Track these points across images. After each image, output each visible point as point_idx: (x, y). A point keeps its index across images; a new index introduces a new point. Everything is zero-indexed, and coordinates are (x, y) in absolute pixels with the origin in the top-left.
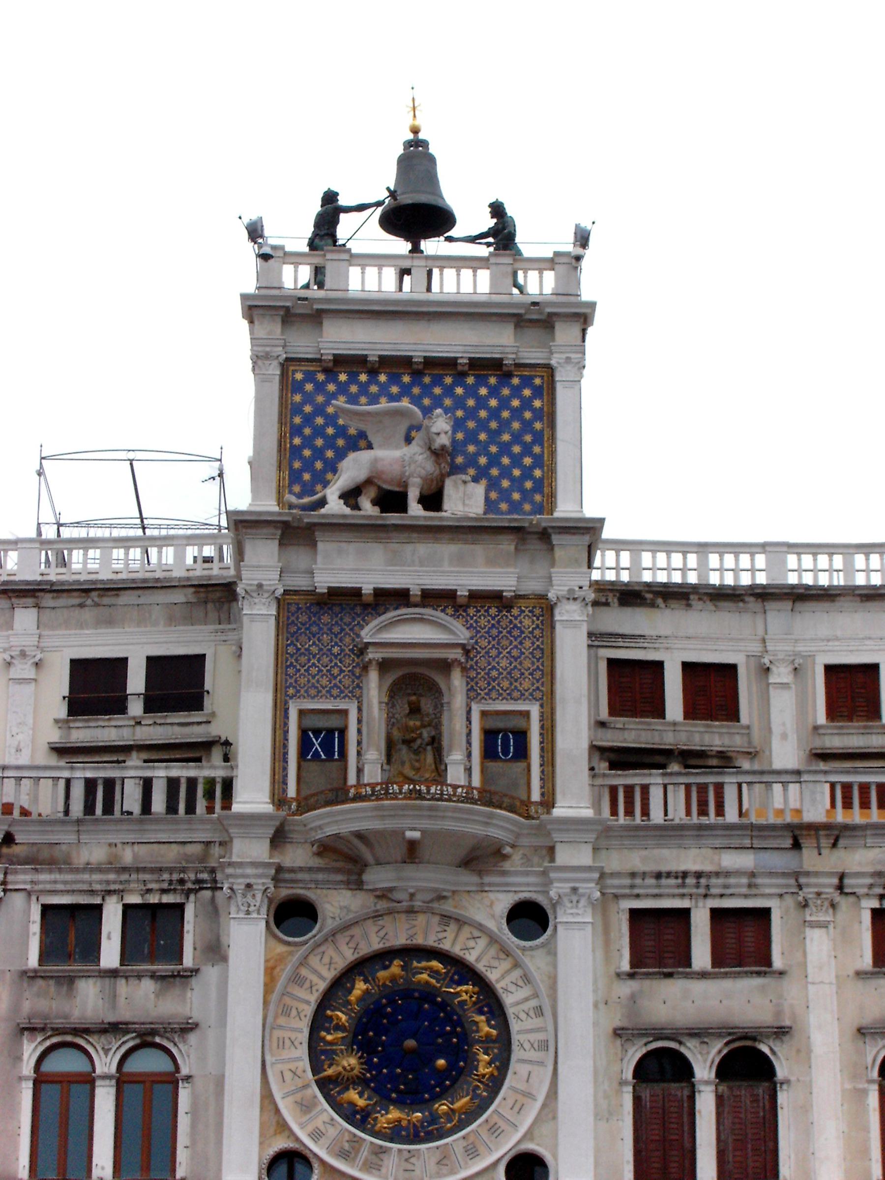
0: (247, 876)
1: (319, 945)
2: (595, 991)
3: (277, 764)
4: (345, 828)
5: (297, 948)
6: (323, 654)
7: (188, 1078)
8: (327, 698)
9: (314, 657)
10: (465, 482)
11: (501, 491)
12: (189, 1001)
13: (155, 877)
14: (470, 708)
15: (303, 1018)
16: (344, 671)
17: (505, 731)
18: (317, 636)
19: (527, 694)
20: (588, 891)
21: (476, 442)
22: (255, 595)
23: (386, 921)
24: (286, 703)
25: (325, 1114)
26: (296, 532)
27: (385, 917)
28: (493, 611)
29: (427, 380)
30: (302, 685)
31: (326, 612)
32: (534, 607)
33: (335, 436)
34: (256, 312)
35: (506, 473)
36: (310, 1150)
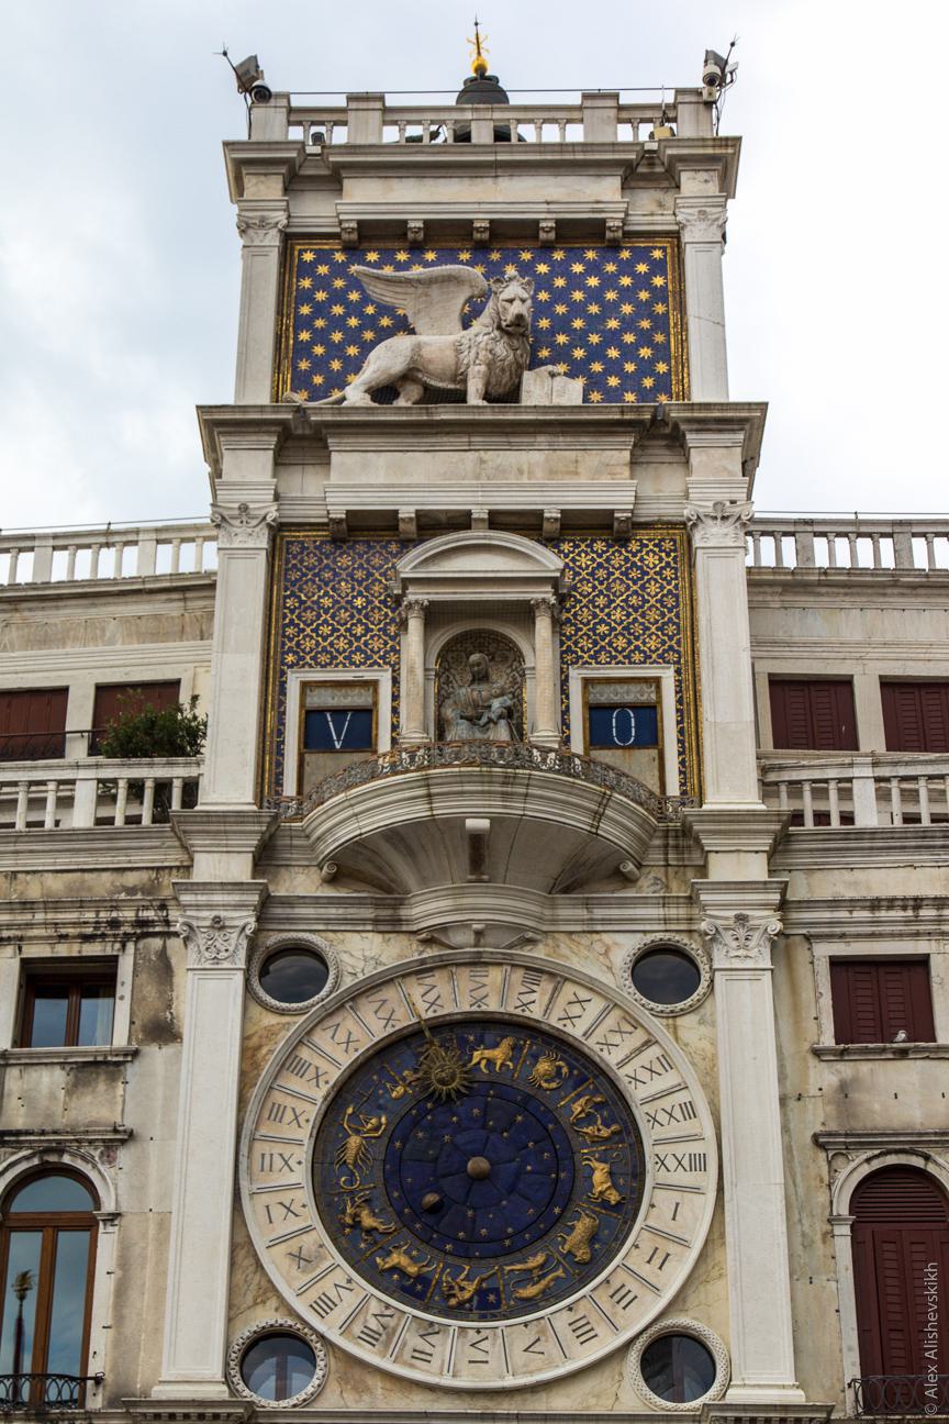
1: (330, 1015)
2: (782, 1077)
3: (267, 758)
6: (340, 608)
7: (113, 1217)
9: (326, 612)
10: (553, 375)
13: (72, 916)
14: (567, 676)
15: (303, 1123)
16: (372, 630)
17: (623, 706)
18: (331, 584)
19: (654, 656)
20: (763, 922)
23: (439, 980)
24: (283, 673)
26: (300, 441)
27: (437, 974)
30: (308, 649)
31: (344, 553)
32: (663, 540)
33: (361, 329)
35: (614, 367)
36: (312, 1328)
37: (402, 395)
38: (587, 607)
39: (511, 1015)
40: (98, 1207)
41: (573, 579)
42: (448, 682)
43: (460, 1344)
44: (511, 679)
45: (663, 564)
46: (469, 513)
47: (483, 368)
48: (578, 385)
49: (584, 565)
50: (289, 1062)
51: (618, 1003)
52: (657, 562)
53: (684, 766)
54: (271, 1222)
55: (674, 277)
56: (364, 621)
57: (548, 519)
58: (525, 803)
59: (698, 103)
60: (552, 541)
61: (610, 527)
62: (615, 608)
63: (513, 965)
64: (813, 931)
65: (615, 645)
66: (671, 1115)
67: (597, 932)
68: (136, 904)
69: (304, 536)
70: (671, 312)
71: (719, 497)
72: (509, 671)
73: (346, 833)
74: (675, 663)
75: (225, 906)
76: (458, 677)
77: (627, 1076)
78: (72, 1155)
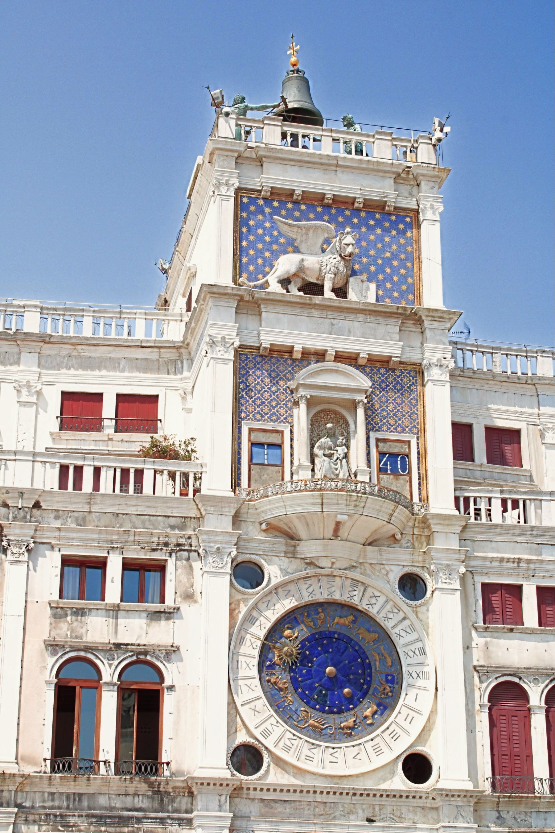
1: (266, 596)
5: (251, 597)
6: (265, 391)
7: (171, 688)
10: (363, 281)
11: (385, 290)
22: (220, 345)
23: (314, 581)
24: (240, 423)
27: (313, 578)
28: (383, 371)
29: (333, 211)
31: (266, 362)
33: (271, 243)
34: (217, 152)
35: (389, 278)
36: (262, 744)
59: (429, 144)
72: (339, 428)
75: (221, 543)
78: (151, 656)
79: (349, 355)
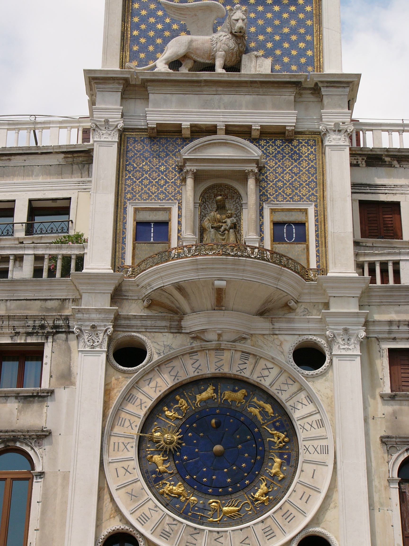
0: (93, 320)
4: (168, 282)
5: (131, 375)
6: (153, 171)
7: (41, 474)
8: (155, 200)
10: (257, 57)
11: (283, 64)
12: (45, 415)
13: (22, 323)
14: (263, 207)
16: (168, 183)
17: (289, 224)
18: (149, 159)
19: (305, 198)
21: (264, 33)
22: (103, 128)
24: (125, 203)
25: (151, 501)
27: (199, 353)
28: (278, 142)
32: (309, 140)
36: (137, 530)
37: (183, 66)
38: (273, 173)
39: (235, 375)
40: (33, 468)
41: (266, 159)
42: (205, 208)
43: (209, 539)
44: (235, 207)
45: (309, 152)
46: (215, 126)
47: (223, 53)
48: (268, 62)
49: (271, 152)
50: (128, 397)
51: (286, 370)
52: (306, 151)
53: (319, 253)
54: (118, 477)
55: (316, 7)
56: (165, 178)
57: (255, 129)
58: (243, 273)
60: (253, 140)
61: (284, 133)
62: (286, 174)
63: (235, 350)
64: (380, 336)
65: (286, 192)
66: (311, 426)
67: (276, 334)
68: (53, 317)
69: (135, 135)
70: (314, 25)
71: (337, 120)
72: (234, 203)
73: (156, 285)
74: (314, 201)
76: (209, 206)
77: (290, 406)
79: (242, 129)
